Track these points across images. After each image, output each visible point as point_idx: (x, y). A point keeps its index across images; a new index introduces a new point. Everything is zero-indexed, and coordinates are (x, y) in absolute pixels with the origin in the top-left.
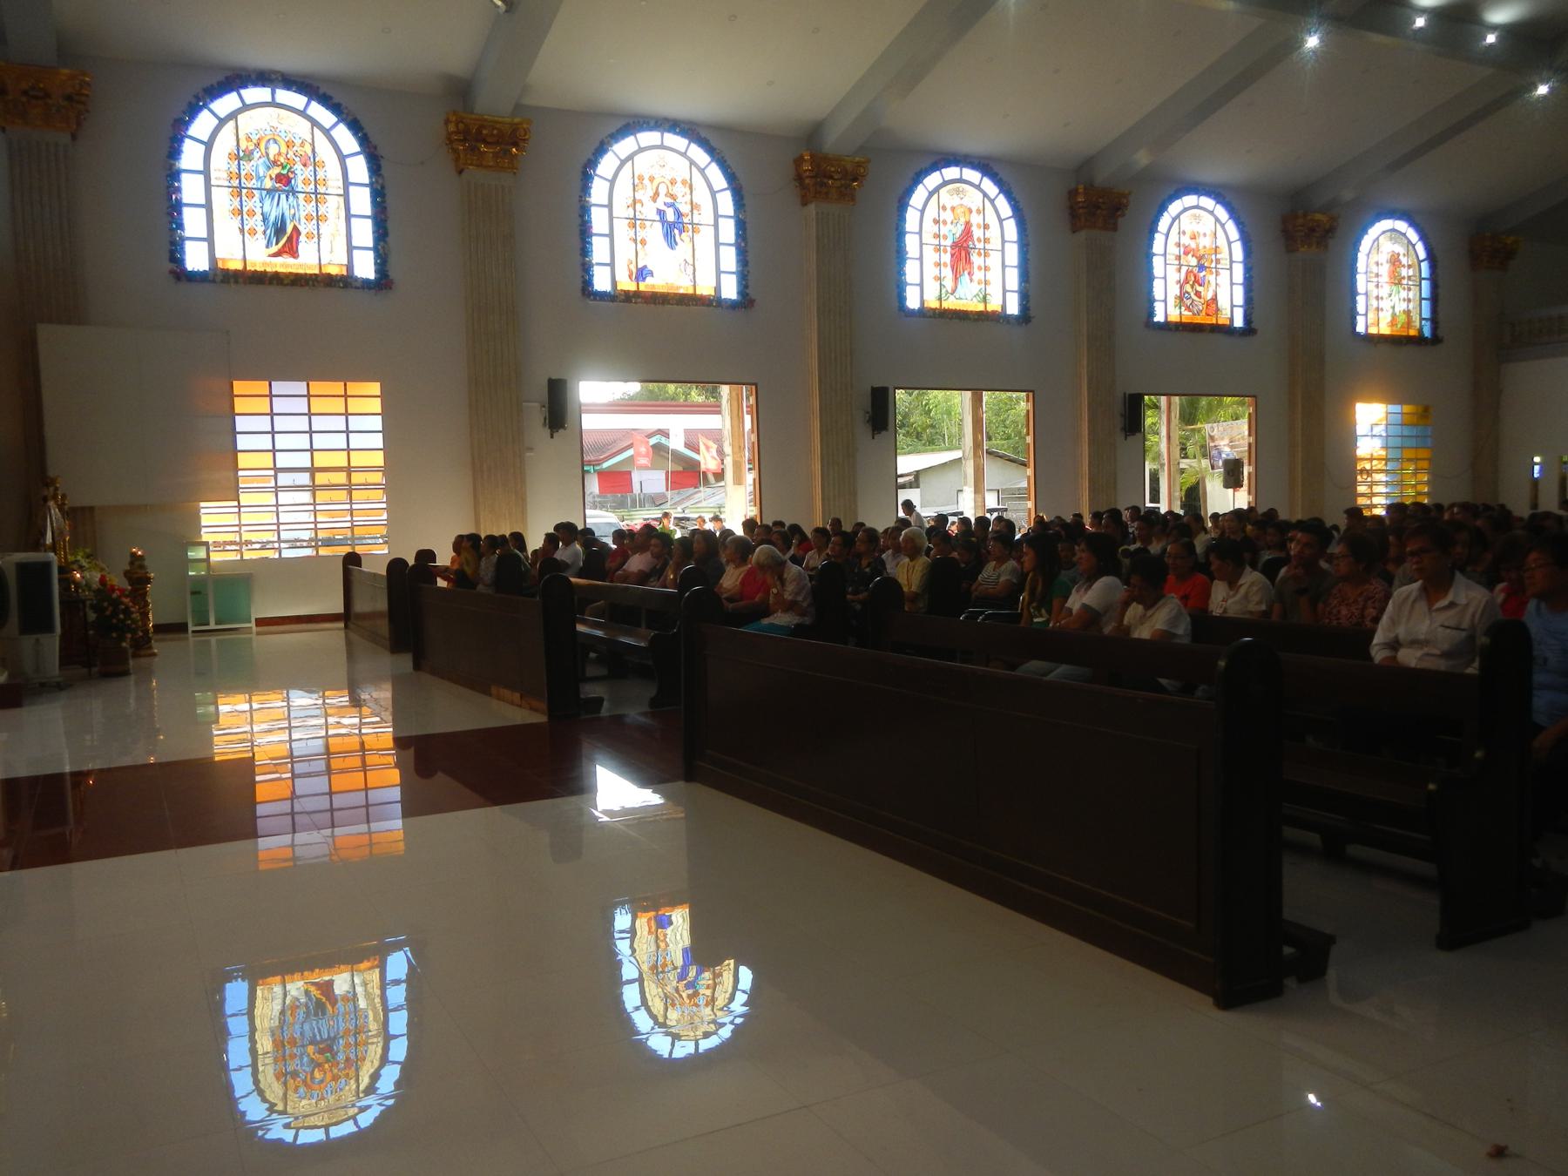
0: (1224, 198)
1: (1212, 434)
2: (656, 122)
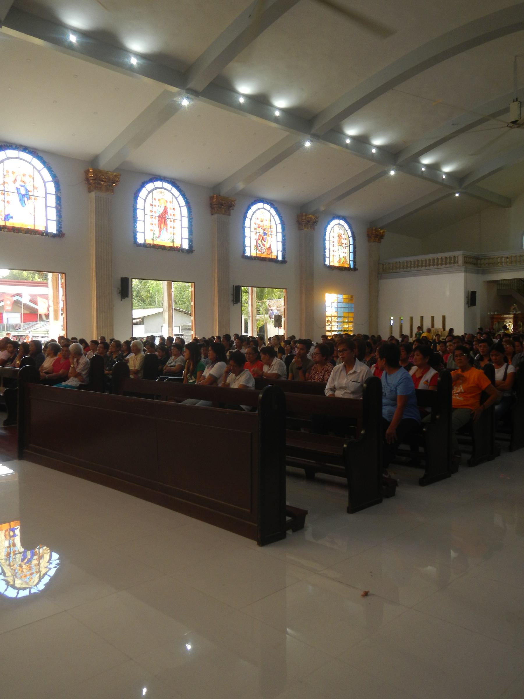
0: (274, 205)
1: (270, 304)
2: (16, 146)
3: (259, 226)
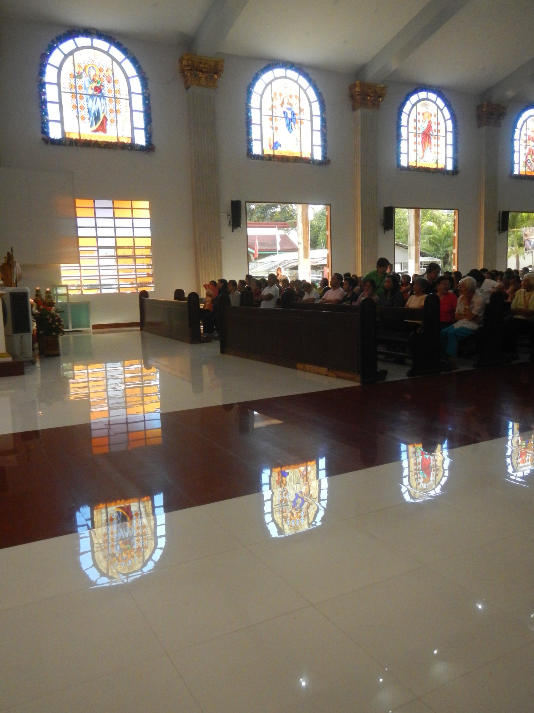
1: (526, 233)
3: (530, 137)
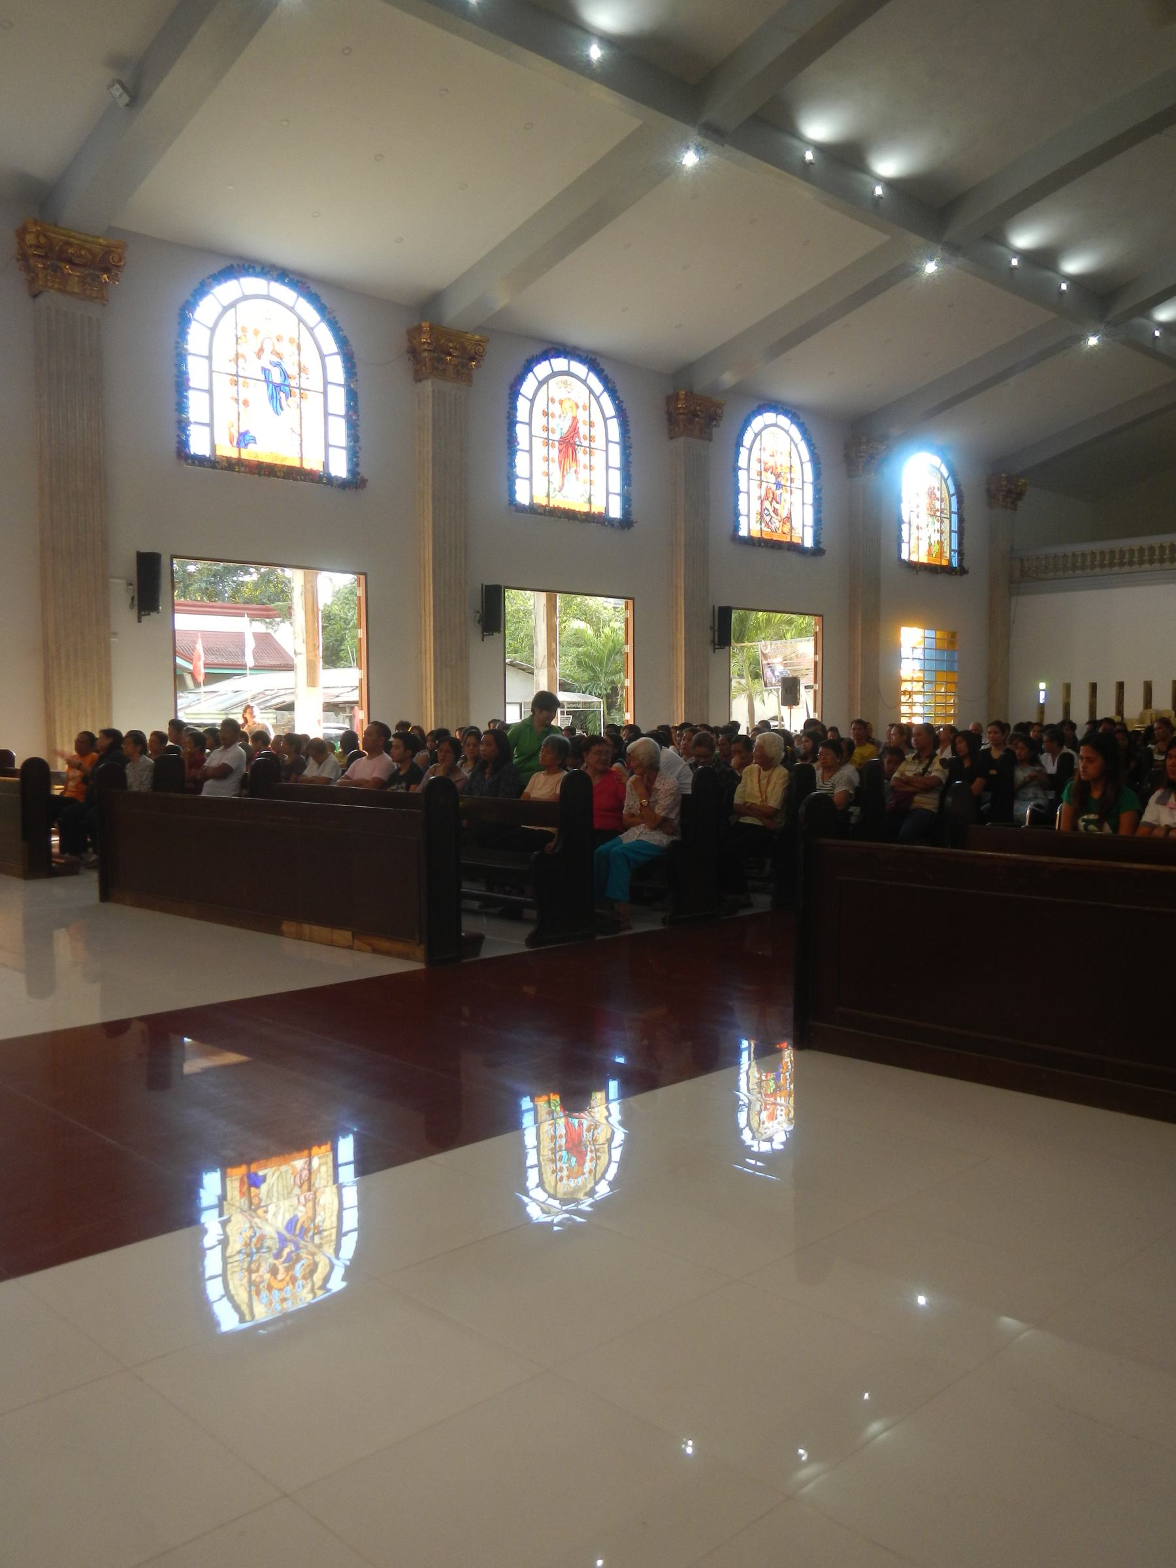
1: (766, 652)
